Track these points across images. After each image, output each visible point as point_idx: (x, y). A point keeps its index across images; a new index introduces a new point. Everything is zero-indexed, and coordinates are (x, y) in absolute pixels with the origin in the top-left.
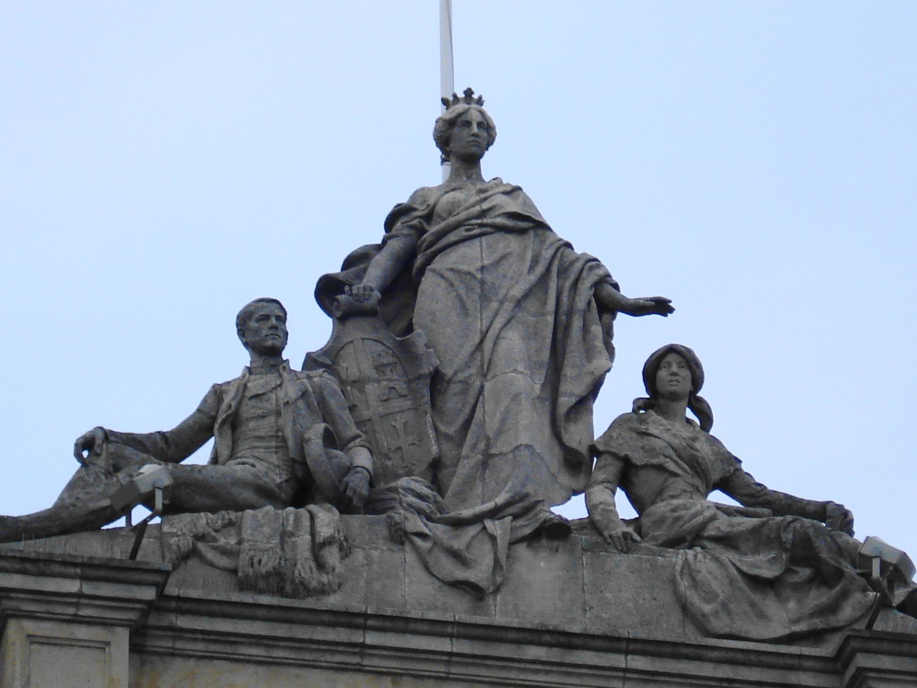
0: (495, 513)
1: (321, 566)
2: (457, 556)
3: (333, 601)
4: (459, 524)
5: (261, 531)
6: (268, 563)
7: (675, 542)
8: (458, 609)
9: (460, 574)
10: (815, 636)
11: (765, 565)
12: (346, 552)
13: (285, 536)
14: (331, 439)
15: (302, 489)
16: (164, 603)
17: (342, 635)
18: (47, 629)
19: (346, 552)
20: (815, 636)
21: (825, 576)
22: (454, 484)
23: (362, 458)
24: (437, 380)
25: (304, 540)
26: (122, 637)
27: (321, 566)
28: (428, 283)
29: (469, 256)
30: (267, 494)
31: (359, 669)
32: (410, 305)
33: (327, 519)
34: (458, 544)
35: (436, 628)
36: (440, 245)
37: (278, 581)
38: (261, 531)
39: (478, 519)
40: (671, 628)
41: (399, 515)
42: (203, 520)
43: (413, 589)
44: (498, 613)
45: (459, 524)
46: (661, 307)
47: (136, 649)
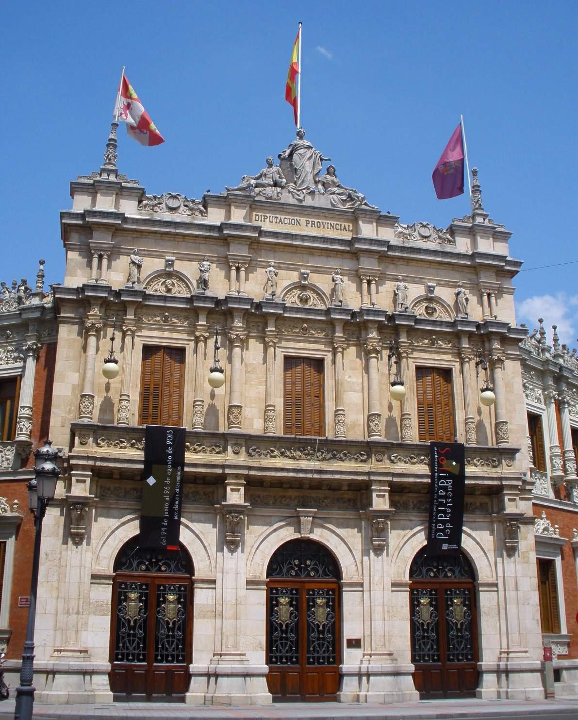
0: (304, 189)
1: (278, 196)
2: (298, 195)
3: (280, 202)
4: (298, 191)
5: (269, 191)
6: (270, 195)
7: (331, 194)
8: (296, 203)
9: (299, 198)
10: (351, 208)
11: (344, 197)
12: (281, 194)
13: (273, 192)
14: (280, 178)
15: (276, 184)
16: (255, 201)
17: (281, 206)
18: (237, 204)
19: (281, 194)
20: (351, 208)
21: (352, 199)
22: (298, 185)
23: (284, 180)
24: (296, 170)
25: (276, 192)
26: (249, 205)
27: (278, 196)
28: (295, 155)
29: (302, 151)
30: (269, 185)
31: (283, 211)
32: (292, 159)
33: (279, 189)
34: (298, 193)
35: (295, 205)
36: (296, 150)
37: (271, 198)
38: (269, 191)
39: (301, 190)
40: (330, 207)
41: (290, 189)
42: (260, 189)
43: (291, 200)
44: (304, 203)
45: (298, 191)
46: (329, 160)
47: (250, 207)
